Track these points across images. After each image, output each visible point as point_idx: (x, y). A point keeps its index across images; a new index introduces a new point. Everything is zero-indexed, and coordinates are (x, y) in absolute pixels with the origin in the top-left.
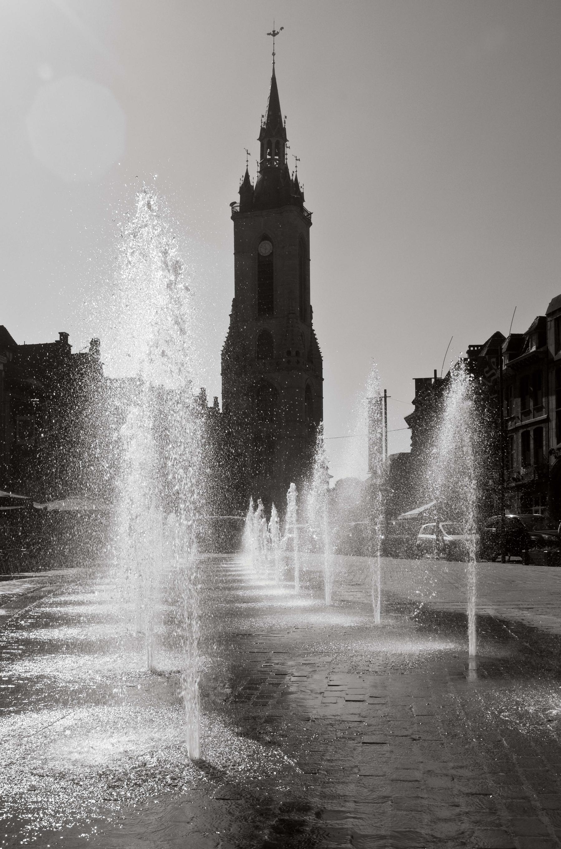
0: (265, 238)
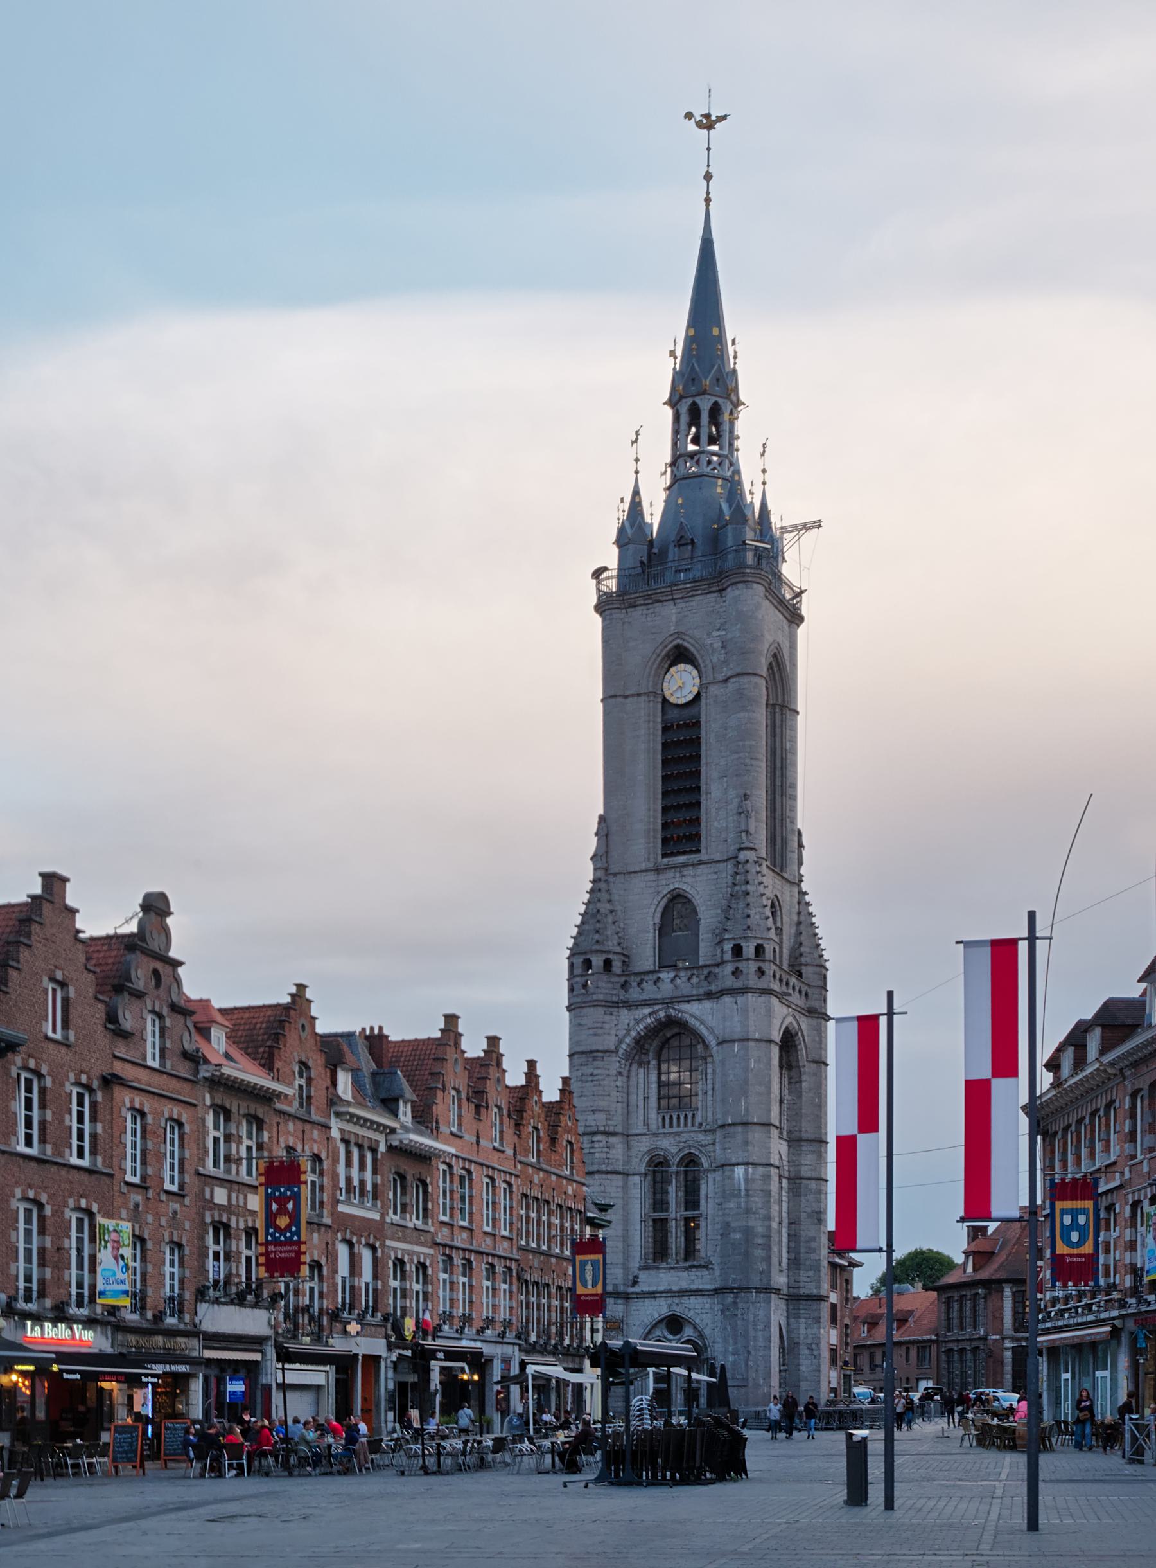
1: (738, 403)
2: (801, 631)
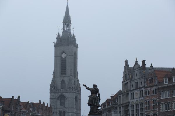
0: (64, 52)
1: (71, 23)
2: (78, 49)
